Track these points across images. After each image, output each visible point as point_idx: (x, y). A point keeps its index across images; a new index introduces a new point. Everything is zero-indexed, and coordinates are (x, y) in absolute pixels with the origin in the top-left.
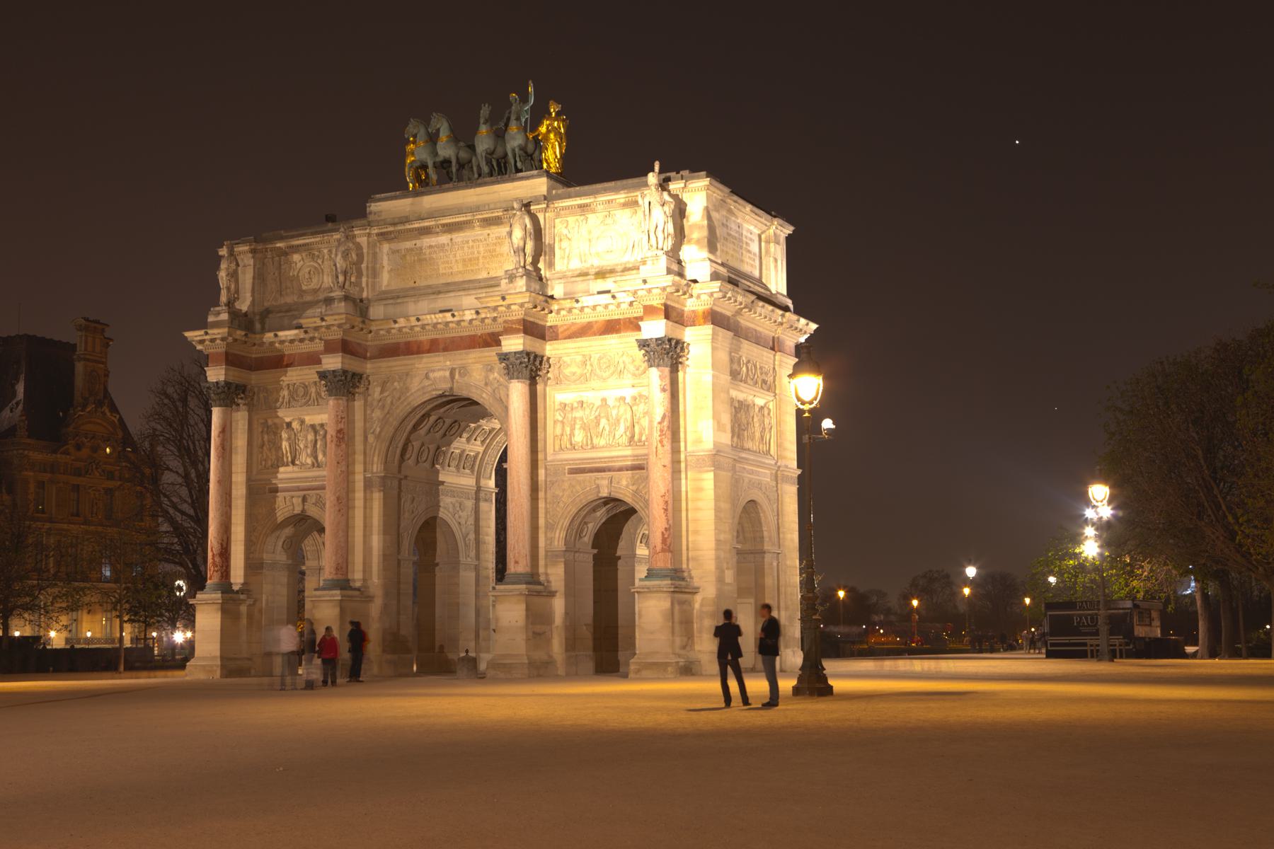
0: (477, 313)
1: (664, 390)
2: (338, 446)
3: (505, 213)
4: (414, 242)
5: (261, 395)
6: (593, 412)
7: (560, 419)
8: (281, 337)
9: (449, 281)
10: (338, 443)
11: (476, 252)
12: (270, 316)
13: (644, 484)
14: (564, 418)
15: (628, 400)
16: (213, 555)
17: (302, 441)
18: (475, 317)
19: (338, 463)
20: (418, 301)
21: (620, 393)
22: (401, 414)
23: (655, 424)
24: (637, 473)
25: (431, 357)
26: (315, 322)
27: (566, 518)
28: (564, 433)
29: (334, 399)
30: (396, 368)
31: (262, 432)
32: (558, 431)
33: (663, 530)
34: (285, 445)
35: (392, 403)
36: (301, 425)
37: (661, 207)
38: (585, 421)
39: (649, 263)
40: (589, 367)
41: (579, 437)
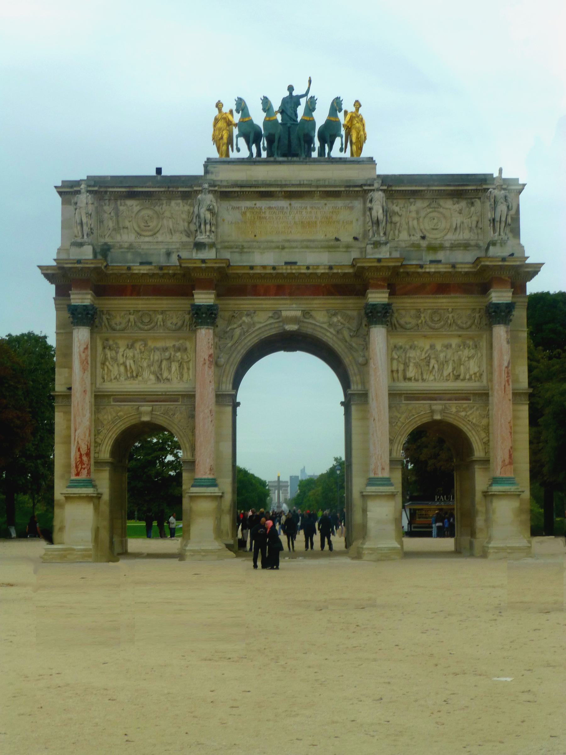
1: (508, 342)
2: (210, 367)
3: (347, 189)
4: (254, 202)
5: (104, 317)
7: (396, 357)
8: (135, 270)
12: (112, 250)
13: (470, 412)
14: (399, 357)
15: (454, 346)
16: (81, 455)
17: (145, 359)
18: (327, 271)
19: (210, 382)
21: (446, 341)
22: (249, 344)
23: (504, 368)
25: (278, 299)
26: (195, 263)
27: (403, 434)
28: (399, 369)
29: (207, 328)
30: (242, 306)
31: (104, 348)
32: (395, 368)
33: (509, 448)
34: (129, 362)
35: (240, 335)
36: (145, 347)
37: (505, 203)
38: (418, 361)
39: (498, 245)
40: (422, 318)
41: (411, 372)
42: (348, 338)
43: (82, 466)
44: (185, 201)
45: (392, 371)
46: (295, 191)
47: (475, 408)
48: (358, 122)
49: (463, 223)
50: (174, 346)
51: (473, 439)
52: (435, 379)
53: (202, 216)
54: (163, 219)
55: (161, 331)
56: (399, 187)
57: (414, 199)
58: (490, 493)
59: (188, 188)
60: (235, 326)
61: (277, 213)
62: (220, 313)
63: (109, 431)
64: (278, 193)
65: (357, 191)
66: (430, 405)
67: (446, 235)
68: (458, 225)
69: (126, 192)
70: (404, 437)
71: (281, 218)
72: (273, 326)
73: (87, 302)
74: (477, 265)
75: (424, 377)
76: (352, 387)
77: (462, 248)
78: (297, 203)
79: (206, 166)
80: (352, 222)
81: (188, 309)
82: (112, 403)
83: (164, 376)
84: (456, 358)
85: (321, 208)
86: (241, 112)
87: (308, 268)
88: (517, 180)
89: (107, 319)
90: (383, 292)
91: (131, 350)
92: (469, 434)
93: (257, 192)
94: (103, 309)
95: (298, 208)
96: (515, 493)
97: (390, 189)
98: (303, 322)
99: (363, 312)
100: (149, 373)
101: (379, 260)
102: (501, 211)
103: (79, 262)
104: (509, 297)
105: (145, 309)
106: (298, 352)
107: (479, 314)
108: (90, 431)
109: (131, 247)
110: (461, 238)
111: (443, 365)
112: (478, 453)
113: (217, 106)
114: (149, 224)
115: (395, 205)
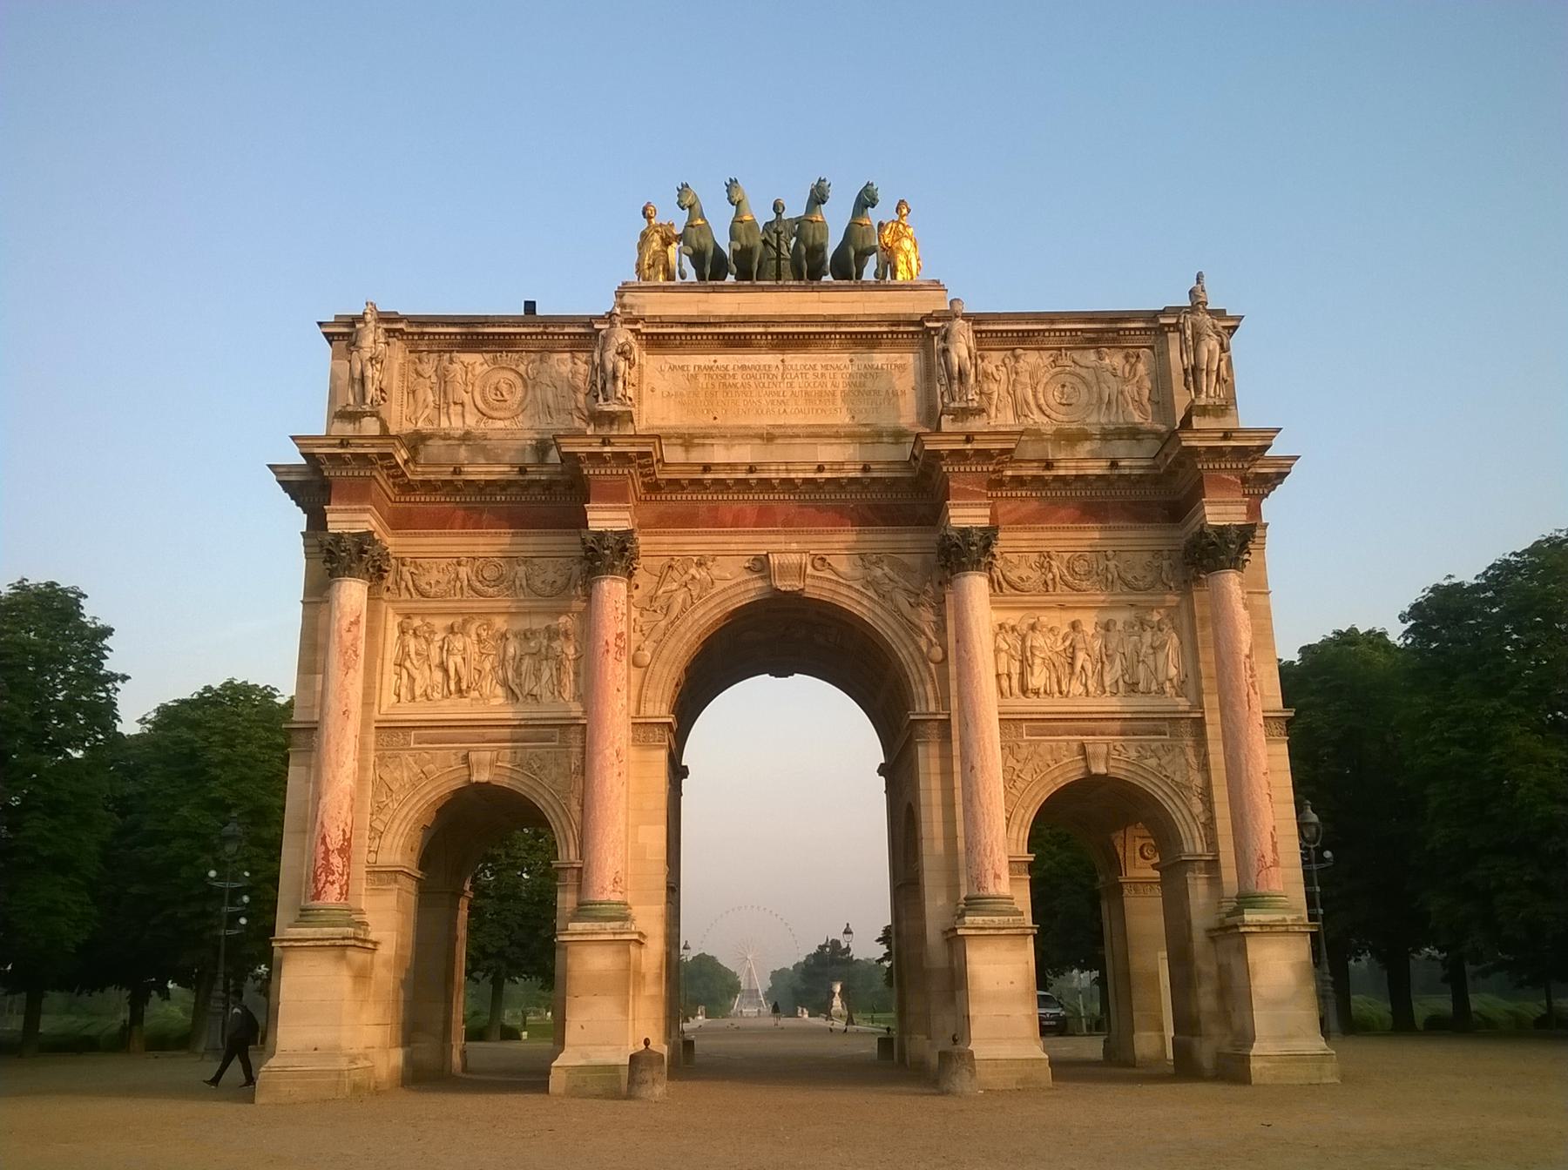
0: (866, 469)
3: (894, 329)
4: (713, 357)
6: (1059, 644)
9: (778, 423)
10: (618, 656)
11: (829, 385)
12: (429, 442)
13: (1170, 757)
15: (1119, 626)
18: (859, 475)
19: (618, 690)
20: (733, 445)
23: (1243, 658)
24: (1154, 740)
25: (762, 533)
28: (1012, 671)
31: (403, 632)
32: (1003, 669)
38: (1050, 654)
40: (1055, 570)
41: (1038, 679)
42: (905, 608)
43: (327, 877)
45: (998, 676)
47: (1177, 750)
49: (1122, 393)
50: (548, 628)
51: (1177, 816)
52: (1087, 691)
53: (609, 367)
54: (534, 387)
55: (522, 597)
57: (1024, 349)
58: (1242, 930)
60: (675, 586)
62: (642, 560)
63: (402, 804)
66: (1083, 747)
67: (1088, 416)
68: (1114, 398)
69: (461, 334)
70: (1031, 809)
71: (766, 385)
72: (751, 586)
73: (360, 528)
74: (1167, 456)
75: (1064, 688)
76: (917, 707)
77: (1125, 437)
78: (796, 360)
79: (620, 294)
81: (579, 554)
82: (412, 746)
83: (525, 694)
84: (1128, 650)
86: (687, 210)
87: (820, 469)
88: (1225, 310)
89: (412, 573)
90: (980, 506)
91: (460, 635)
92: (1168, 805)
94: (403, 555)
96: (1297, 929)
97: (976, 327)
98: (813, 577)
99: (933, 558)
100: (494, 682)
101: (969, 438)
102: (1209, 351)
103: (344, 442)
104: (1241, 513)
105: (492, 555)
106: (796, 675)
107: (1168, 562)
108: (352, 799)
109: (467, 437)
110: (1121, 420)
111: (1103, 663)
112: (1194, 845)
113: (644, 213)
114: (507, 397)
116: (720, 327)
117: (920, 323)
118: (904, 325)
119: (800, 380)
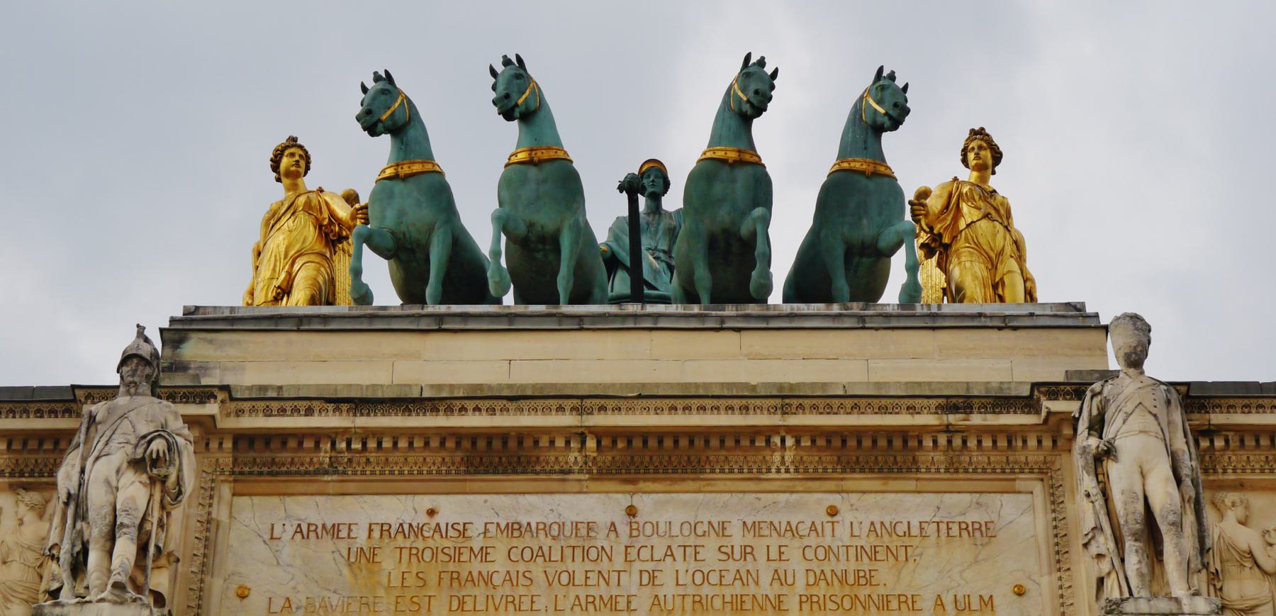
3: (953, 419)
4: (426, 502)
11: (765, 578)
44: (34, 497)
46: (661, 435)
48: (987, 216)
53: (97, 497)
56: (1247, 409)
59: (53, 413)
61: (556, 556)
64: (560, 443)
65: (1010, 434)
71: (580, 578)
80: (988, 603)
85: (803, 530)
93: (445, 435)
95: (676, 531)
113: (275, 165)
115: (1232, 516)
116: (449, 411)
117: (1028, 403)
118: (984, 409)
119: (680, 565)
